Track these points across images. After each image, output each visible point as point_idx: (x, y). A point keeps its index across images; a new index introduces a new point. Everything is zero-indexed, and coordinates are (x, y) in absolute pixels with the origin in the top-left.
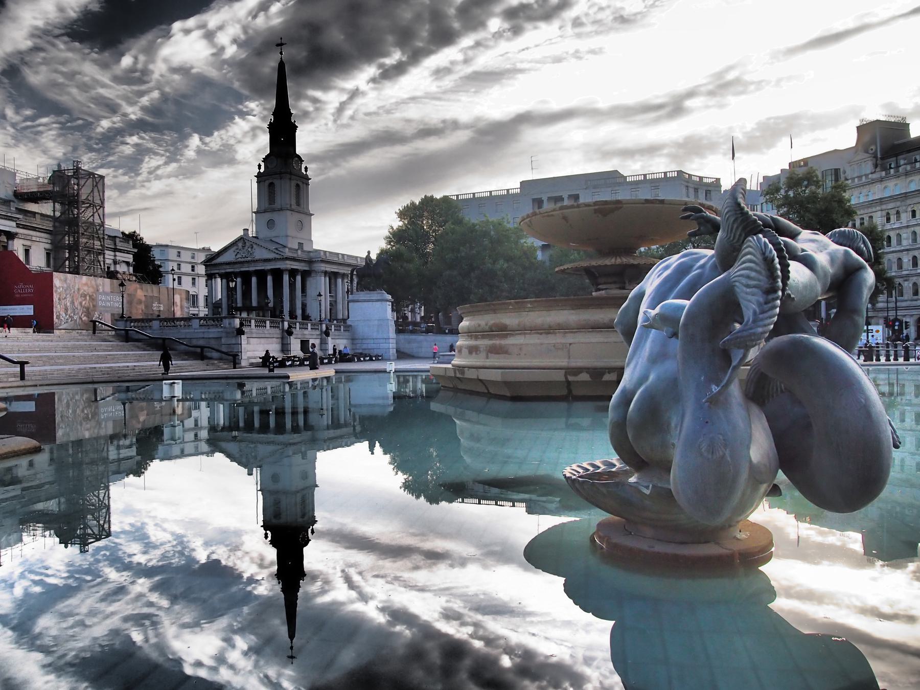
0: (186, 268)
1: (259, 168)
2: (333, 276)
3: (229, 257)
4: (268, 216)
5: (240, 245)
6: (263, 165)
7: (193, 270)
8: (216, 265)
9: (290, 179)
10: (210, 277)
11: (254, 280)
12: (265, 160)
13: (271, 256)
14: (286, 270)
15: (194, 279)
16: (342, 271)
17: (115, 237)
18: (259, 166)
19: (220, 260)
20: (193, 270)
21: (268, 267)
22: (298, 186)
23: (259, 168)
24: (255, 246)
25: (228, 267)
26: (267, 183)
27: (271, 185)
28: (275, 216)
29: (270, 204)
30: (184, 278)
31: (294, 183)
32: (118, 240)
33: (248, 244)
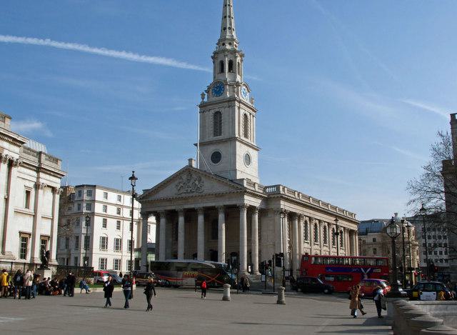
0: (112, 211)
2: (292, 216)
3: (170, 192)
4: (212, 149)
5: (185, 177)
7: (119, 213)
8: (152, 202)
9: (239, 108)
10: (145, 215)
11: (201, 219)
14: (243, 206)
15: (119, 222)
17: (40, 153)
19: (162, 194)
20: (119, 213)
21: (220, 203)
22: (245, 115)
24: (203, 179)
25: (168, 203)
26: (213, 112)
27: (218, 115)
28: (222, 149)
29: (215, 134)
30: (109, 220)
31: (242, 112)
32: (43, 157)
33: (194, 176)
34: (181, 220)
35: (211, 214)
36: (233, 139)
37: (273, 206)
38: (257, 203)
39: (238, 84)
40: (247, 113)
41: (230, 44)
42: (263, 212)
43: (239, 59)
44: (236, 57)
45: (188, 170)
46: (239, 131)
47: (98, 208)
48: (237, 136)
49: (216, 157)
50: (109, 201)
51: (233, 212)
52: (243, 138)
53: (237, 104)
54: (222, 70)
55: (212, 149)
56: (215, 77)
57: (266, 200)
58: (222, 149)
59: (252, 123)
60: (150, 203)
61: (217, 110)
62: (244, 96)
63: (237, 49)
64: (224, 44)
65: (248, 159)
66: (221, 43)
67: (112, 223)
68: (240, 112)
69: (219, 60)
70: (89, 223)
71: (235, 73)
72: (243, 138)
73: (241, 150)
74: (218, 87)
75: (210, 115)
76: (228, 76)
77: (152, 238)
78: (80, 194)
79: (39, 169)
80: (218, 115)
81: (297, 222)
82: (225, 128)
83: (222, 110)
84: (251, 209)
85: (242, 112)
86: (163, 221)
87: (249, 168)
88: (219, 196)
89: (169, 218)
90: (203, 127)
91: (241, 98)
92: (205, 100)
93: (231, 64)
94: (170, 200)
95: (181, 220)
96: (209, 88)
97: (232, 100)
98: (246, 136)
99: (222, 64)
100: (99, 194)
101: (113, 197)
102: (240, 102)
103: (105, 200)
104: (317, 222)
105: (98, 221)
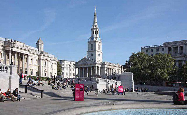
0: (68, 66)
2: (108, 68)
4: (91, 53)
13: (92, 63)
16: (110, 68)
18: (89, 39)
19: (79, 64)
21: (91, 66)
31: (98, 44)
34: (83, 69)
35: (89, 68)
36: (95, 51)
37: (103, 66)
38: (100, 66)
39: (97, 37)
42: (101, 68)
43: (97, 30)
44: (96, 30)
45: (85, 59)
46: (97, 49)
47: (65, 66)
49: (92, 55)
50: (68, 64)
51: (93, 68)
53: (96, 42)
54: (93, 34)
55: (91, 53)
57: (102, 65)
58: (93, 53)
59: (101, 46)
60: (76, 65)
65: (99, 55)
67: (68, 69)
68: (97, 44)
70: (64, 69)
73: (97, 53)
74: (92, 38)
75: (90, 45)
76: (95, 35)
77: (77, 73)
78: (61, 62)
79: (53, 60)
81: (110, 70)
82: (94, 48)
84: (98, 67)
86: (79, 69)
87: (99, 58)
88: (91, 64)
89: (81, 69)
90: (89, 47)
93: (95, 31)
94: (81, 65)
95: (83, 69)
97: (95, 41)
98: (99, 50)
99: (93, 32)
100: (65, 62)
101: (69, 63)
103: (67, 64)
104: (116, 70)
105: (65, 69)
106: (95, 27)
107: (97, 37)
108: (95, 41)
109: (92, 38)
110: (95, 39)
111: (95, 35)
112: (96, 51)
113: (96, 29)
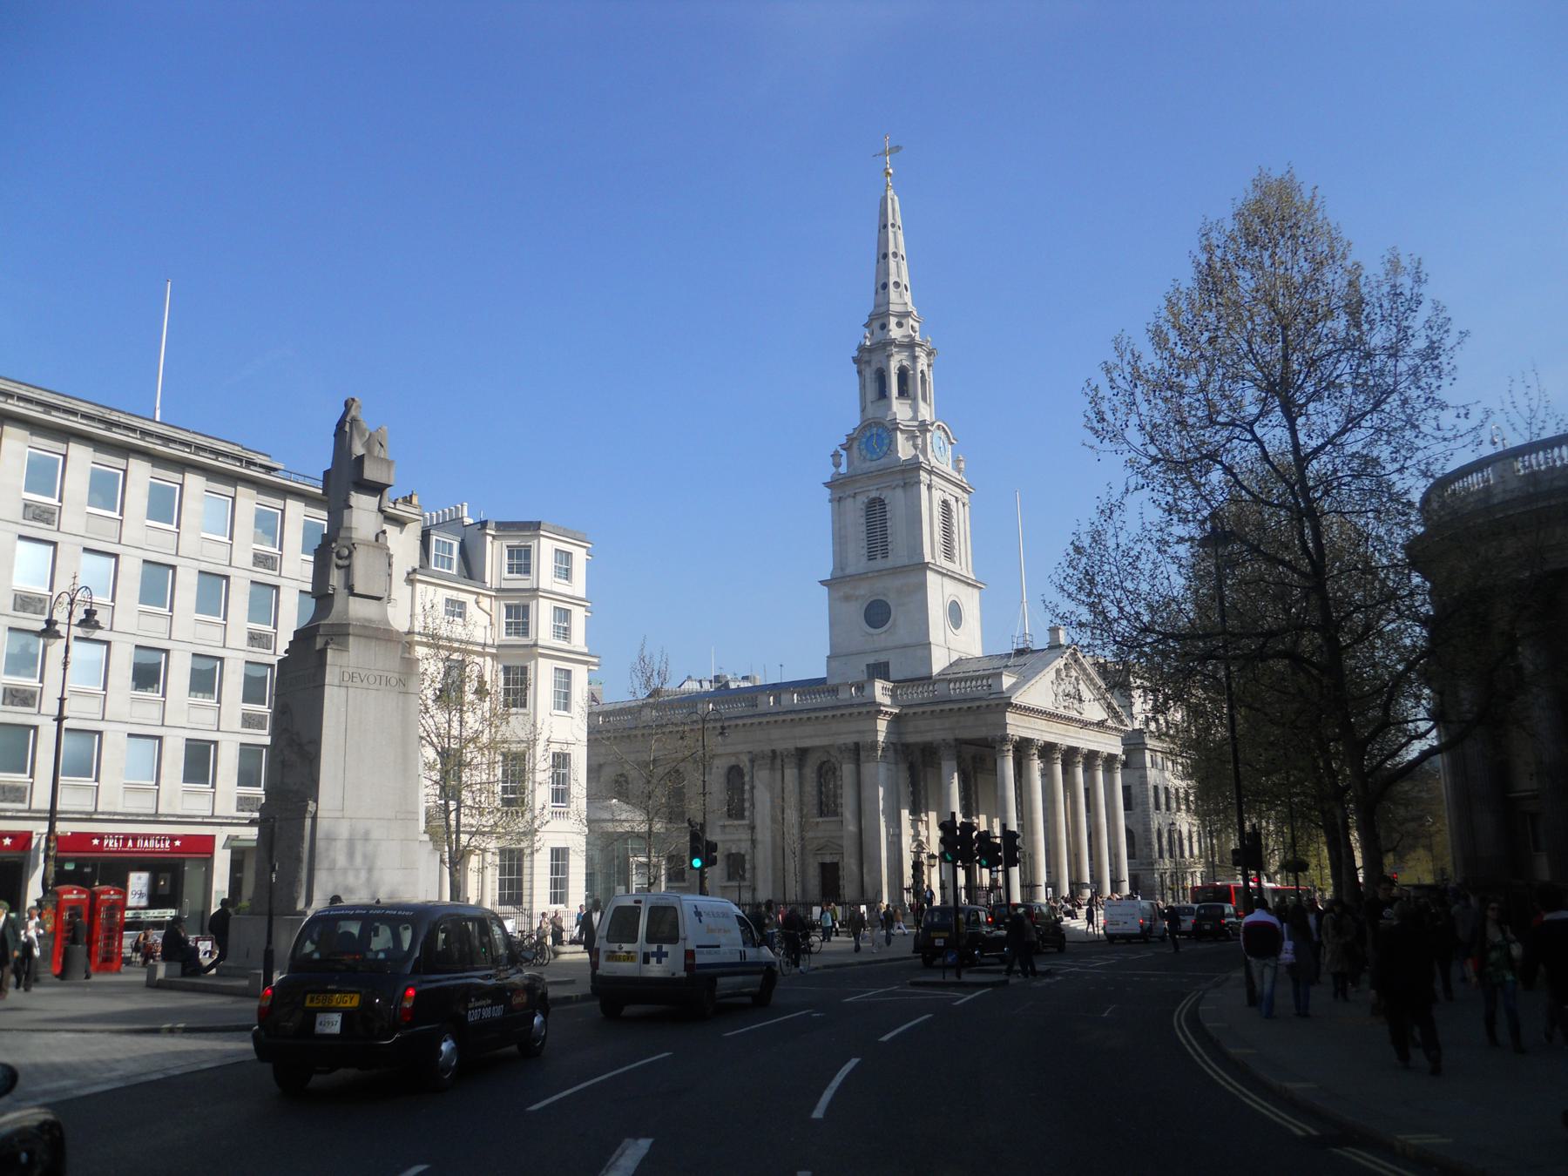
1: (837, 465)
6: (843, 453)
9: (929, 487)
12: (847, 447)
22: (945, 503)
23: (837, 465)
26: (862, 499)
29: (871, 558)
31: (938, 496)
39: (924, 427)
40: (948, 498)
41: (900, 325)
43: (922, 363)
44: (914, 358)
46: (931, 549)
48: (928, 558)
49: (877, 614)
52: (942, 561)
53: (924, 476)
54: (883, 393)
55: (865, 591)
56: (863, 410)
59: (961, 516)
61: (874, 494)
62: (939, 454)
63: (918, 338)
64: (884, 327)
65: (955, 614)
66: (876, 325)
68: (930, 501)
69: (875, 366)
71: (915, 399)
72: (942, 561)
73: (938, 592)
80: (876, 510)
83: (887, 495)
85: (938, 496)
90: (839, 539)
91: (934, 462)
92: (843, 469)
93: (903, 374)
96: (850, 439)
97: (914, 467)
98: (949, 554)
99: (882, 377)
102: (930, 472)
106: (895, 333)
107: (924, 427)
108: (914, 467)
109: (874, 434)
110: (904, 450)
111: (900, 410)
112: (925, 566)
113: (910, 346)
